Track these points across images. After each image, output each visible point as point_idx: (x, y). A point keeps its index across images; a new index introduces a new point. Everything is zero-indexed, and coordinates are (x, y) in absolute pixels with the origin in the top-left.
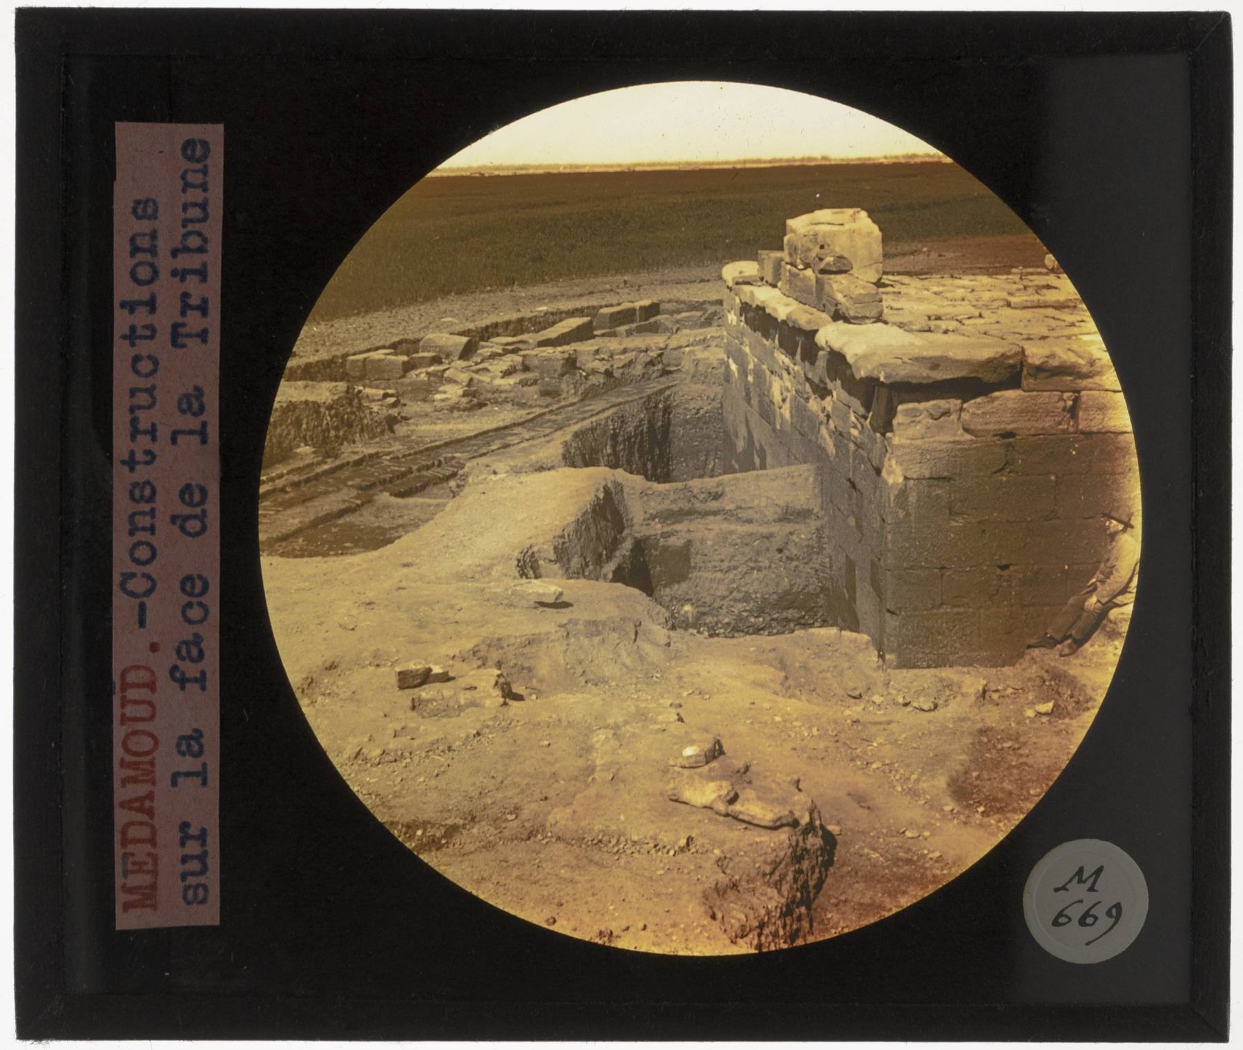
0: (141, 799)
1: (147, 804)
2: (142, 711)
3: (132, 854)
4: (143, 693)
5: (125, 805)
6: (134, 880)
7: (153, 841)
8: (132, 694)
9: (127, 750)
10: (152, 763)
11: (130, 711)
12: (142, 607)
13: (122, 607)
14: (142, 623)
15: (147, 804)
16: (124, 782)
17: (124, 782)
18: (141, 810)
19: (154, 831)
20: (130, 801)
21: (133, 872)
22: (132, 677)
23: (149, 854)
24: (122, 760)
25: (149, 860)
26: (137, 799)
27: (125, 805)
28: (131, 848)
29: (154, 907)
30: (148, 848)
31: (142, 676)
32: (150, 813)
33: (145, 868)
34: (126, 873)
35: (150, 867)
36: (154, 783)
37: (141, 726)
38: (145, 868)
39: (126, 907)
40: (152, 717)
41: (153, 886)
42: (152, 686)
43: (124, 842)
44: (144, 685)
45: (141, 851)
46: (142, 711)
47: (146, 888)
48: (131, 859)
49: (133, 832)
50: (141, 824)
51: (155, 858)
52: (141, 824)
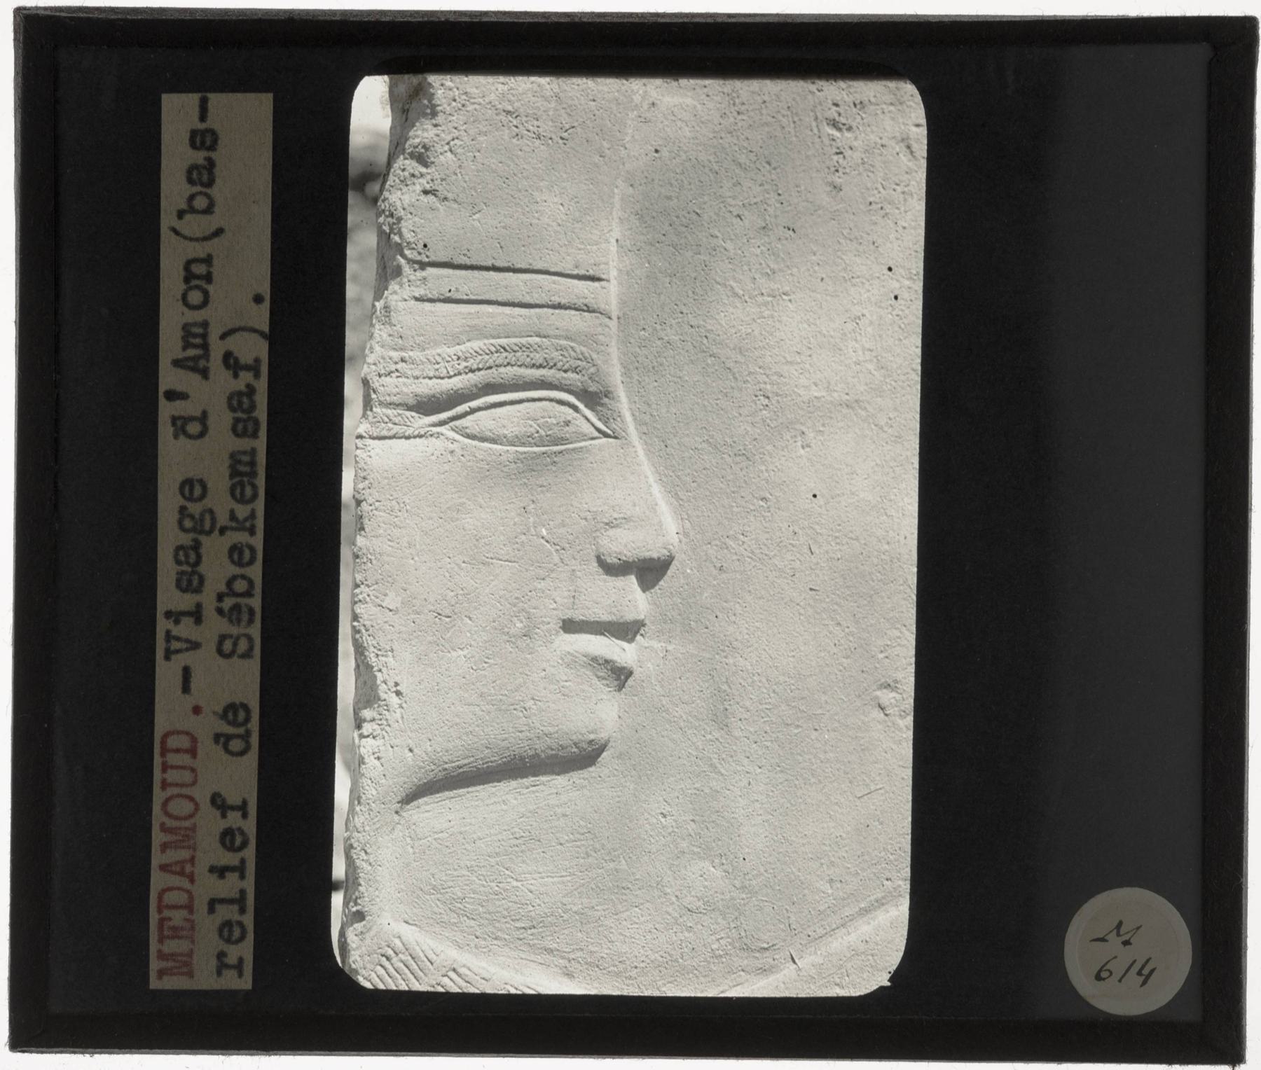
0: (182, 863)
2: (187, 776)
3: (170, 919)
4: (185, 759)
5: (163, 868)
6: (171, 946)
7: (190, 908)
8: (173, 759)
9: (167, 814)
10: (193, 829)
11: (172, 776)
12: (187, 672)
13: (166, 674)
14: (186, 688)
16: (164, 847)
17: (164, 847)
18: (182, 873)
20: (170, 865)
21: (168, 937)
22: (173, 742)
24: (163, 824)
26: (177, 863)
27: (163, 868)
28: (166, 913)
29: (190, 974)
30: (184, 913)
31: (185, 742)
34: (161, 940)
37: (185, 791)
39: (161, 973)
40: (194, 783)
41: (190, 954)
42: (193, 752)
43: (160, 911)
44: (186, 751)
45: (178, 917)
46: (187, 776)
47: (181, 955)
48: (167, 924)
49: (171, 898)
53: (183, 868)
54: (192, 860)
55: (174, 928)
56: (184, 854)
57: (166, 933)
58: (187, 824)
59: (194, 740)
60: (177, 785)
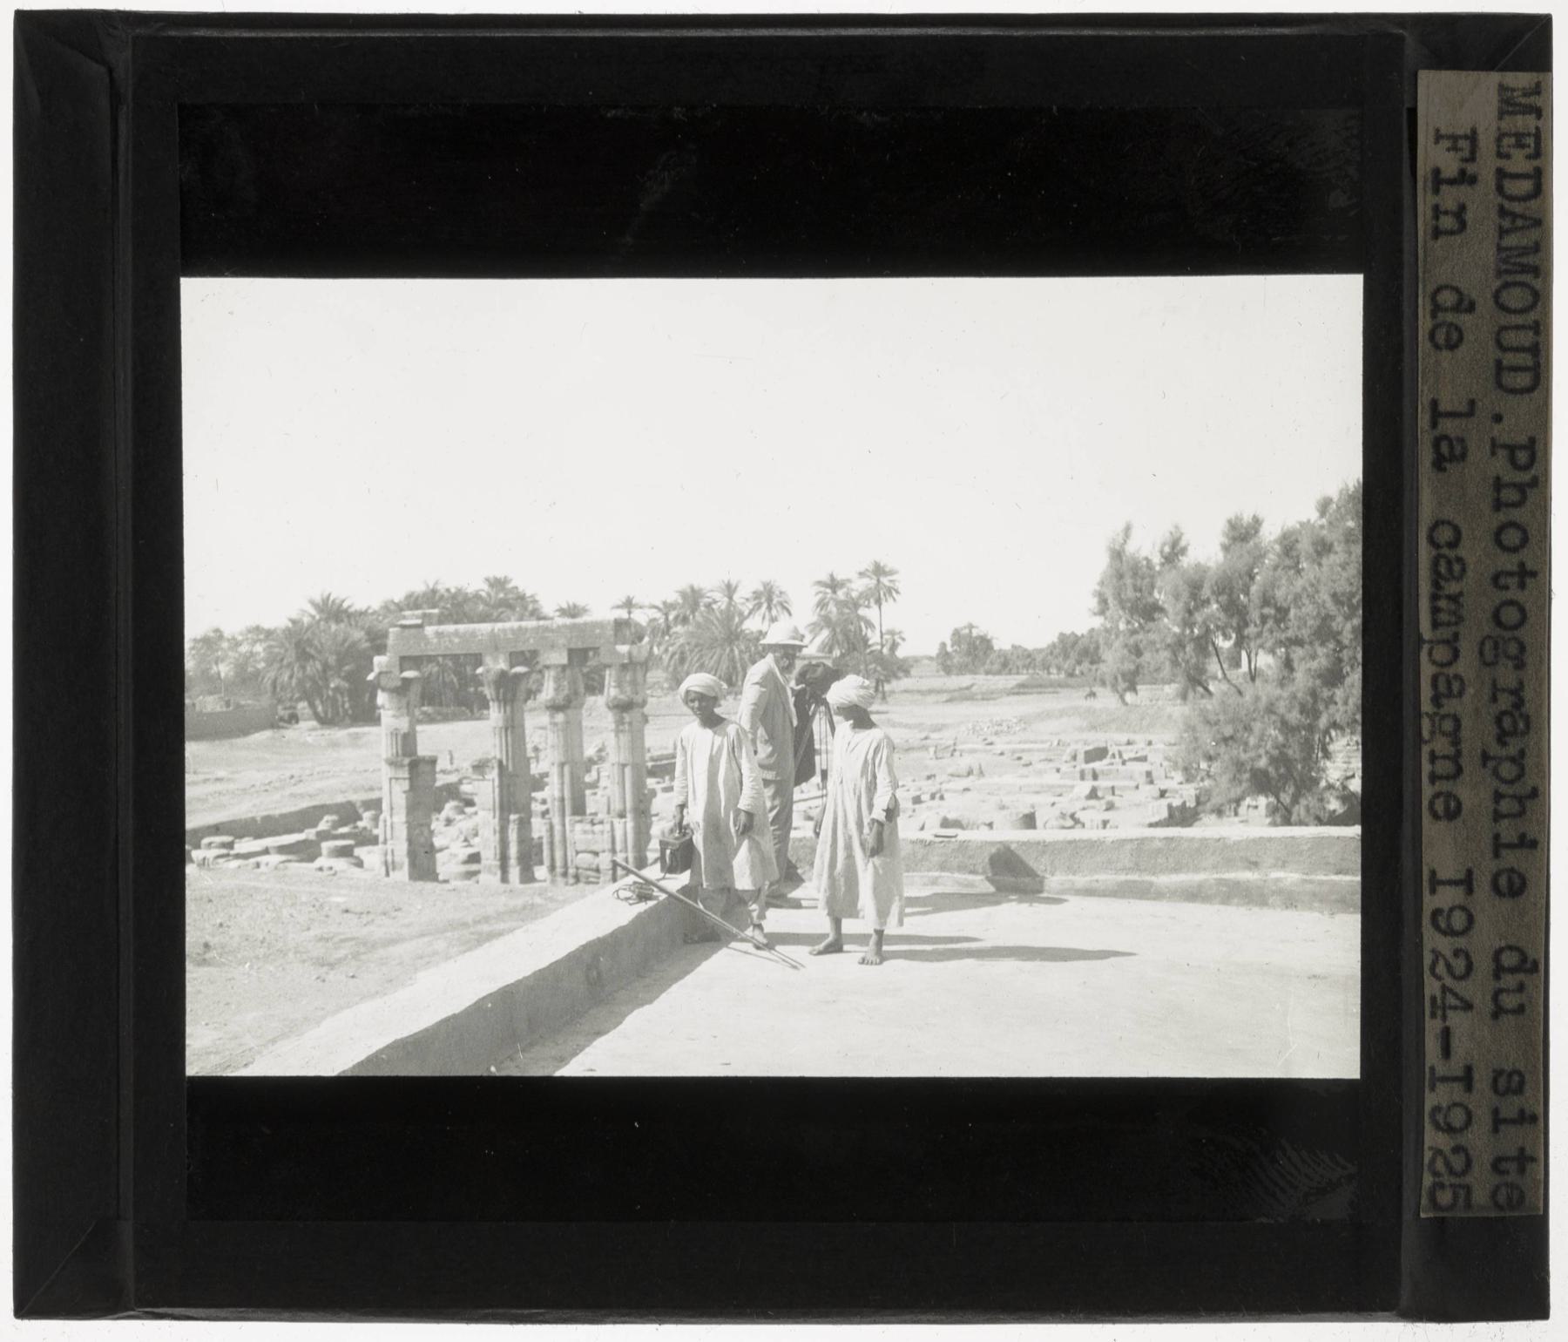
0: (1517, 229)
1: (1506, 224)
2: (1511, 338)
3: (1529, 157)
4: (1510, 359)
7: (1501, 174)
15: (1506, 224)
18: (1514, 216)
19: (1500, 189)
23: (1508, 156)
25: (1505, 150)
31: (1510, 379)
32: (1503, 212)
33: (1513, 140)
35: (1506, 141)
36: (1500, 249)
38: (1513, 140)
48: (1531, 151)
50: (1512, 198)
51: (1500, 155)
52: (1512, 198)
53: (1513, 222)
54: (1503, 232)
55: (1520, 145)
56: (1511, 240)
57: (1531, 141)
58: (1509, 278)
59: (1500, 385)
60: (1518, 327)
